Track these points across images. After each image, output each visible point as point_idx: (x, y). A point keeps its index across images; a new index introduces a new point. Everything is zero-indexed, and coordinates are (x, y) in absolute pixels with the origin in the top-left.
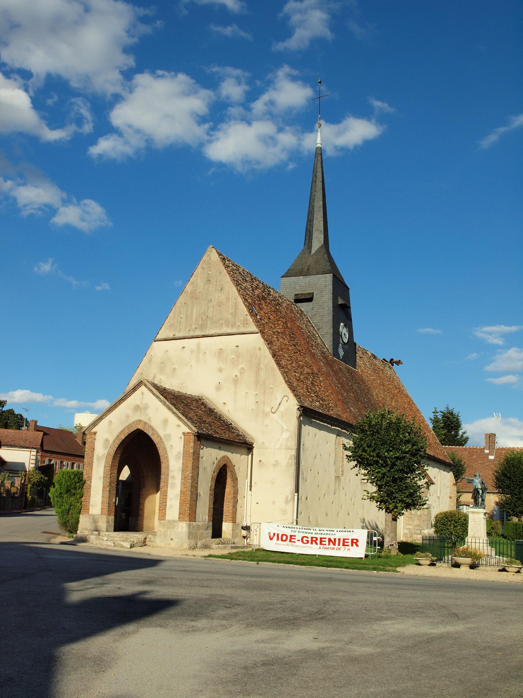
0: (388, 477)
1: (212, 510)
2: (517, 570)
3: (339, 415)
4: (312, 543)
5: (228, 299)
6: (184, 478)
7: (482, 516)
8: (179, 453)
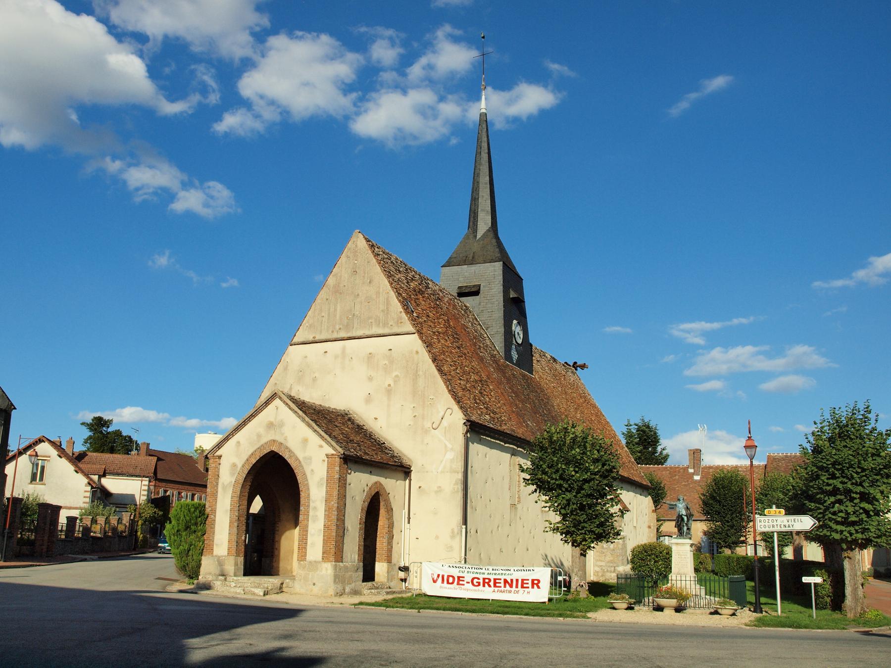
0: (574, 504)
1: (362, 548)
2: (731, 612)
3: (513, 431)
4: (484, 586)
5: (378, 293)
6: (328, 510)
7: (688, 548)
8: (322, 479)
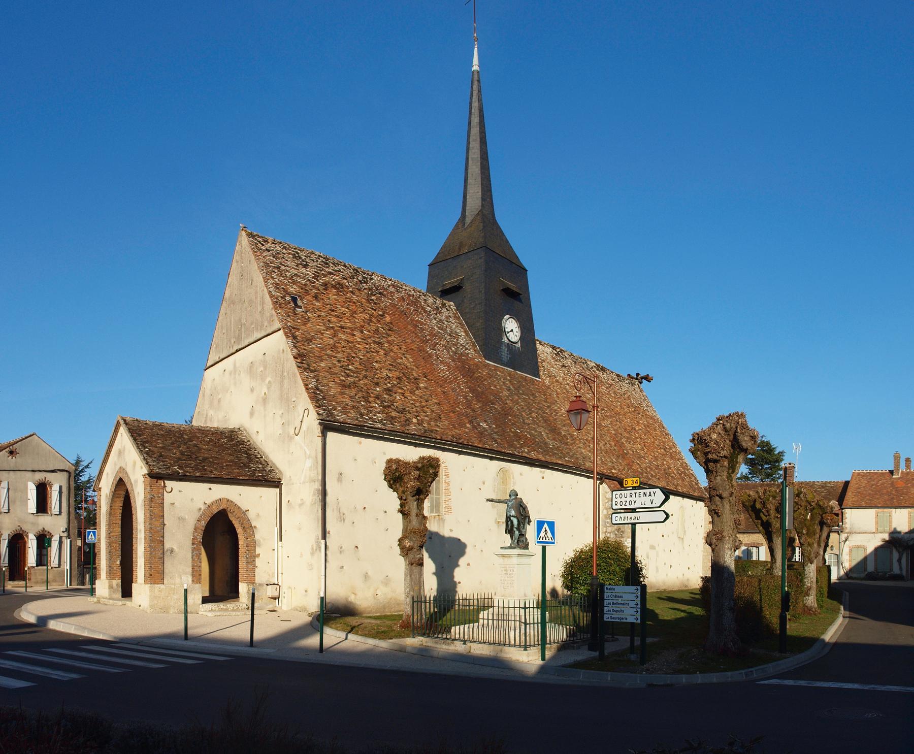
5: (256, 293)
